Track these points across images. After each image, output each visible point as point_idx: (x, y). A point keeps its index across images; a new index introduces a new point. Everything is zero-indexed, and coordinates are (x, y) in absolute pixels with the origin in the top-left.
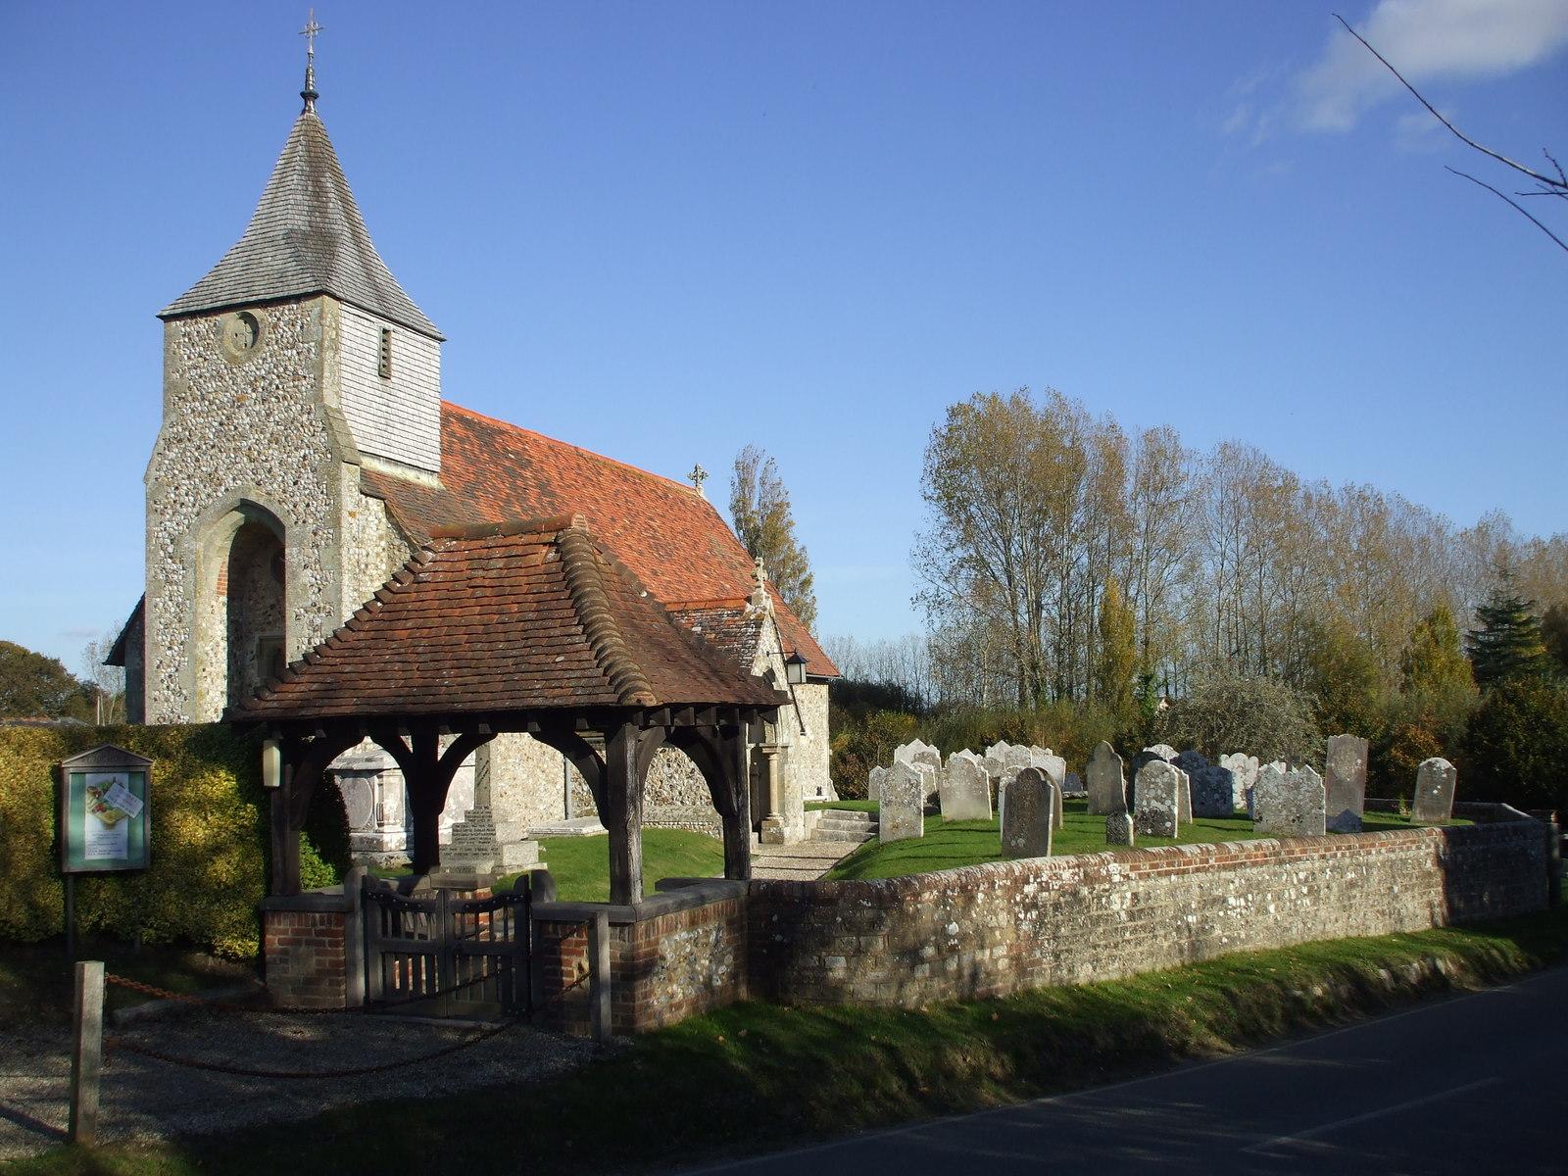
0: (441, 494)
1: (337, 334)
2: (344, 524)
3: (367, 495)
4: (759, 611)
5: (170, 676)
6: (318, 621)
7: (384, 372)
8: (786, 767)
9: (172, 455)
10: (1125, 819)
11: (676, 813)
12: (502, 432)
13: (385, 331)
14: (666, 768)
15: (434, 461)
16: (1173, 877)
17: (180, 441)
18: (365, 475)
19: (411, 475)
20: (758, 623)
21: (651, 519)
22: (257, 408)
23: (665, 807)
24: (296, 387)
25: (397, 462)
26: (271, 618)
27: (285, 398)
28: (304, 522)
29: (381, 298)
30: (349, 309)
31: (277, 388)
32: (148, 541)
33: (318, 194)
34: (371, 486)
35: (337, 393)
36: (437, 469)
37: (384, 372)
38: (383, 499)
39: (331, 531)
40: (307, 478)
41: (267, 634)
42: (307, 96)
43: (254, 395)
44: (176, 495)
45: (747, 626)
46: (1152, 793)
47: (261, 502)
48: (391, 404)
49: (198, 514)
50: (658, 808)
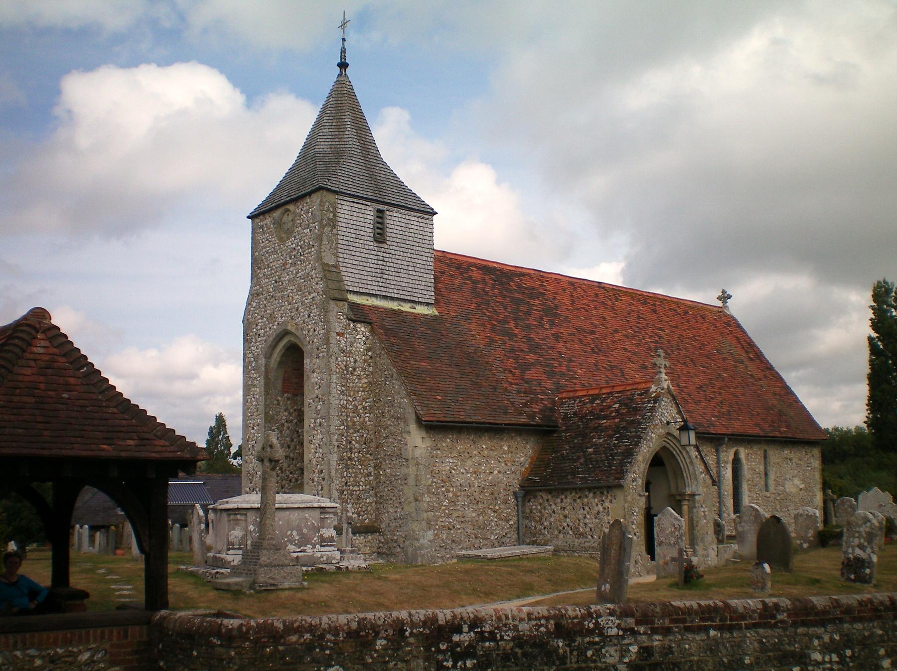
0: (434, 317)
1: (335, 216)
2: (333, 341)
3: (354, 321)
4: (659, 390)
6: (319, 407)
7: (380, 236)
8: (695, 510)
10: (763, 568)
11: (587, 544)
12: (523, 275)
13: (379, 211)
14: (582, 511)
15: (430, 296)
16: (712, 633)
18: (353, 306)
19: (406, 308)
20: (656, 400)
21: (661, 329)
23: (582, 540)
25: (392, 299)
29: (378, 189)
30: (345, 198)
32: (244, 360)
33: (340, 127)
34: (358, 314)
35: (334, 254)
36: (433, 302)
37: (380, 236)
38: (370, 323)
40: (315, 311)
42: (343, 65)
45: (649, 402)
46: (856, 541)
48: (386, 259)
50: (577, 540)
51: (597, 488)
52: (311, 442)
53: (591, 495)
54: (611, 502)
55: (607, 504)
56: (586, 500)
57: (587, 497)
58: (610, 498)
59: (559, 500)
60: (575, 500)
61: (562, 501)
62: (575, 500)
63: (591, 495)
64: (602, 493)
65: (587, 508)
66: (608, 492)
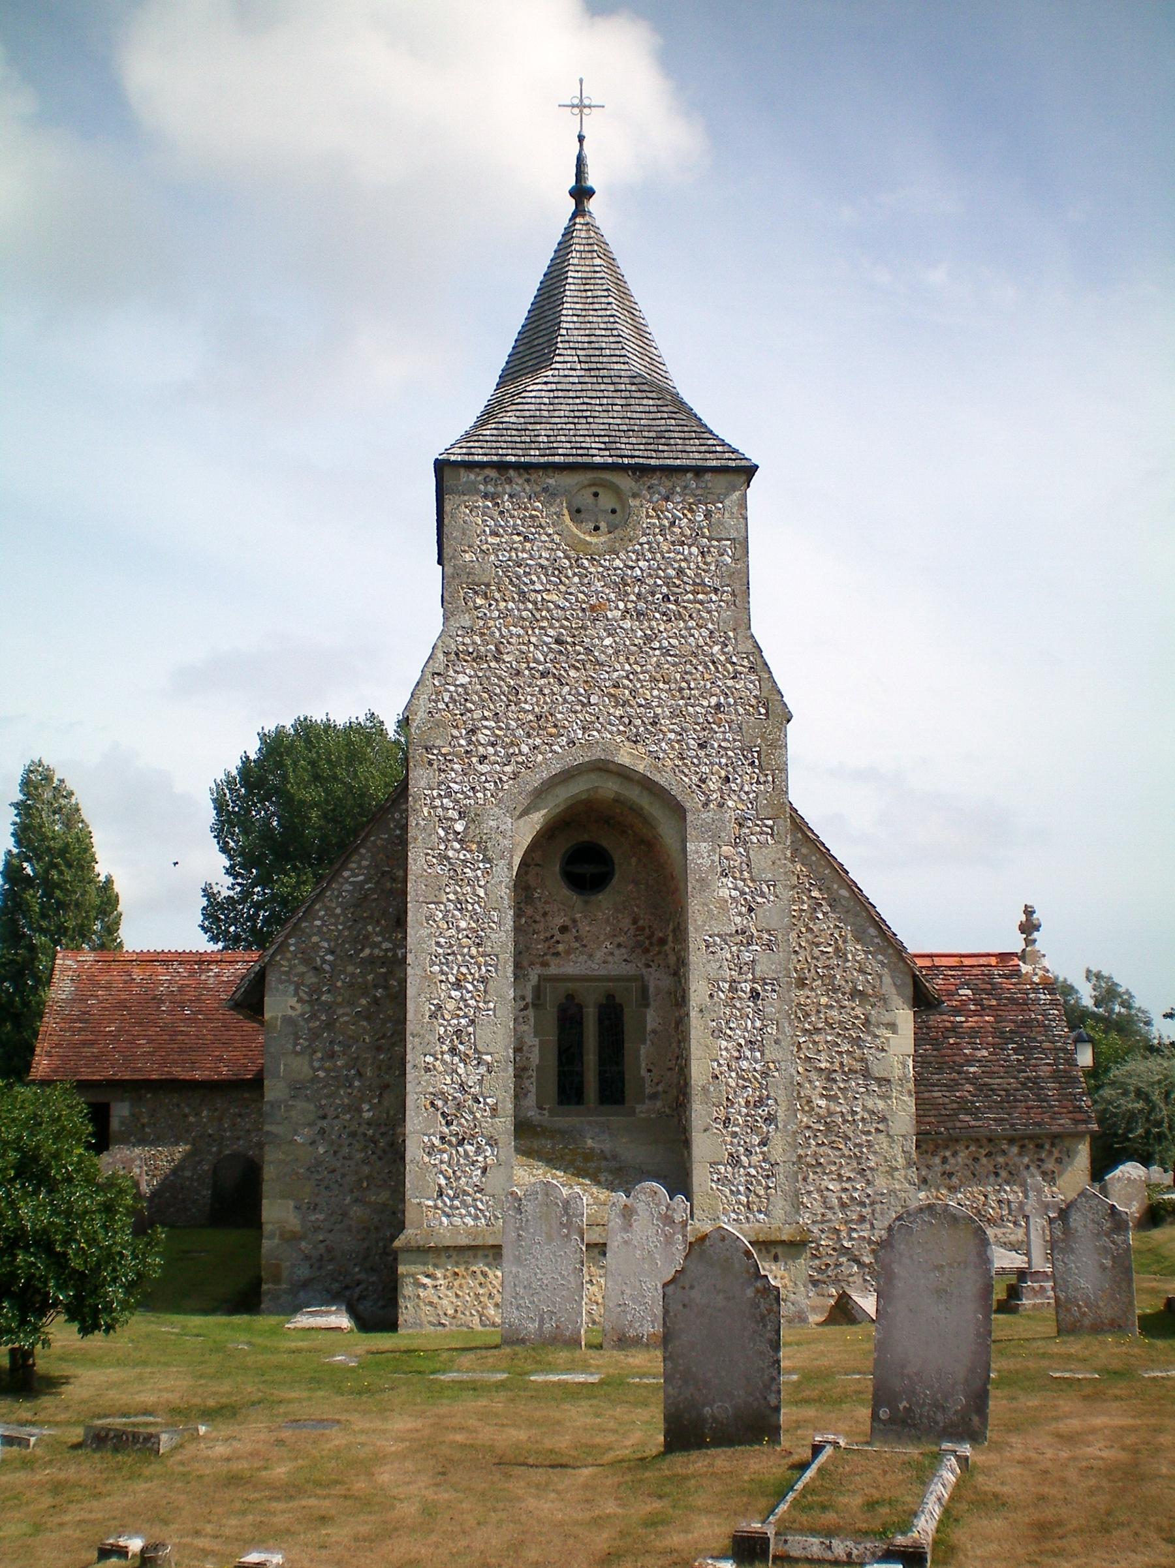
5: (458, 1033)
9: (463, 679)
17: (479, 658)
22: (627, 624)
24: (701, 603)
26: (561, 947)
27: (680, 617)
28: (721, 805)
31: (666, 598)
39: (770, 822)
41: (553, 970)
43: (621, 605)
44: (470, 743)
47: (640, 768)
49: (515, 776)
51: (1031, 1138)
52: (717, 1033)
53: (1015, 1150)
54: (1059, 1161)
55: (1050, 1165)
56: (1001, 1160)
57: (1004, 1153)
58: (1056, 1154)
59: (937, 1160)
60: (976, 1160)
61: (944, 1160)
62: (976, 1160)
63: (1015, 1150)
64: (1039, 1146)
65: (1004, 1174)
66: (1053, 1145)
